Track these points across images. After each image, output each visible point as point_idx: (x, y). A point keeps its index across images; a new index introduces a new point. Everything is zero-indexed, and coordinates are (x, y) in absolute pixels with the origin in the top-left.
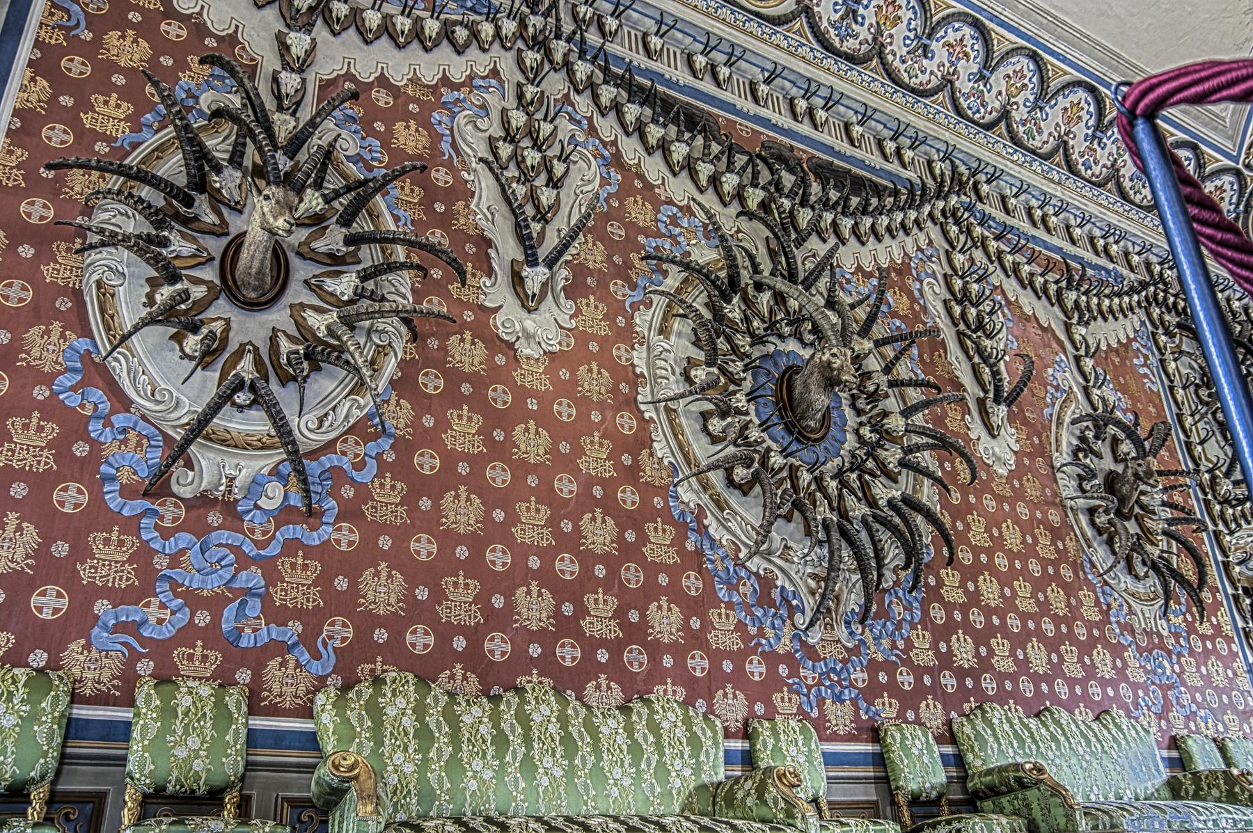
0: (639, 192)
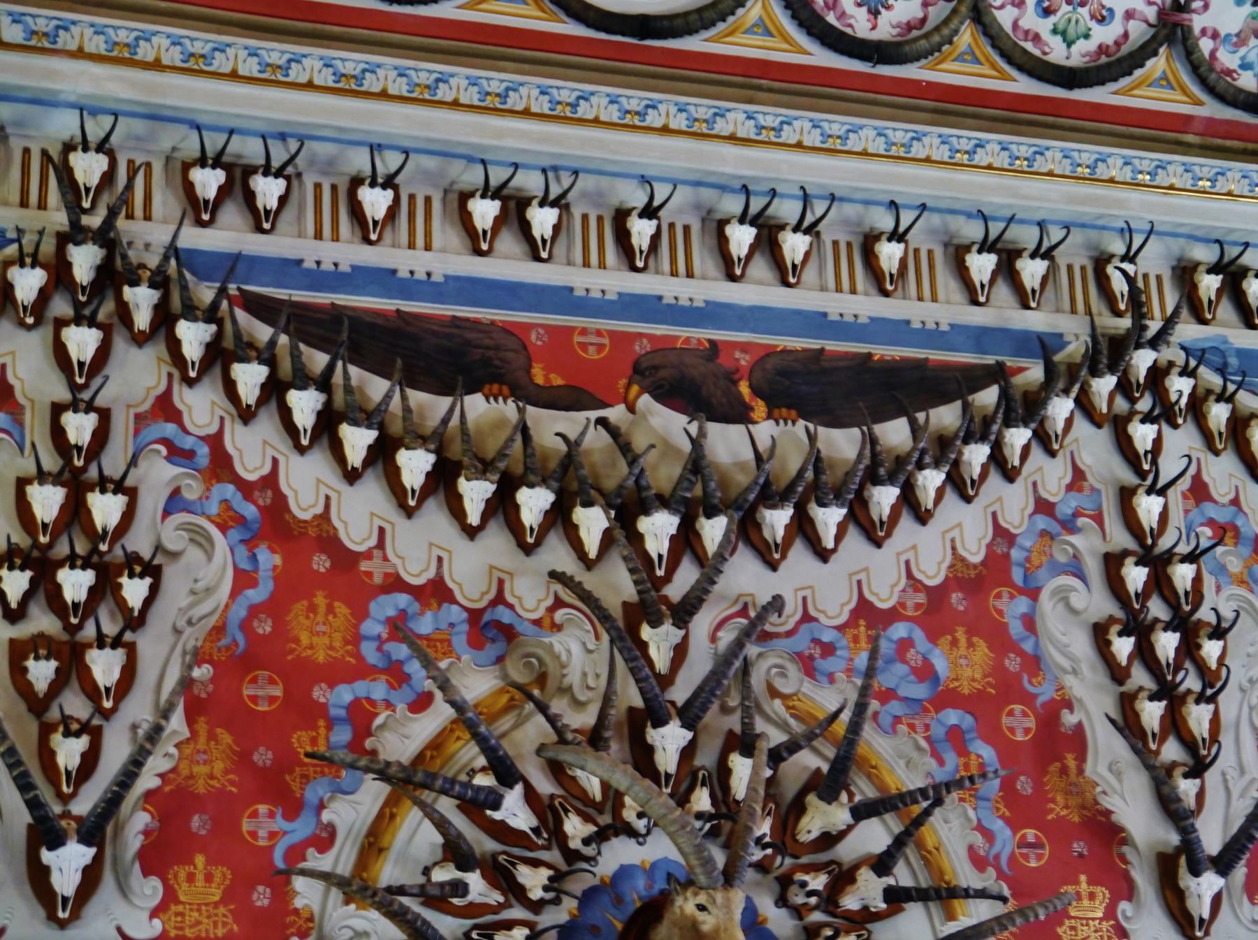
0: (322, 581)
